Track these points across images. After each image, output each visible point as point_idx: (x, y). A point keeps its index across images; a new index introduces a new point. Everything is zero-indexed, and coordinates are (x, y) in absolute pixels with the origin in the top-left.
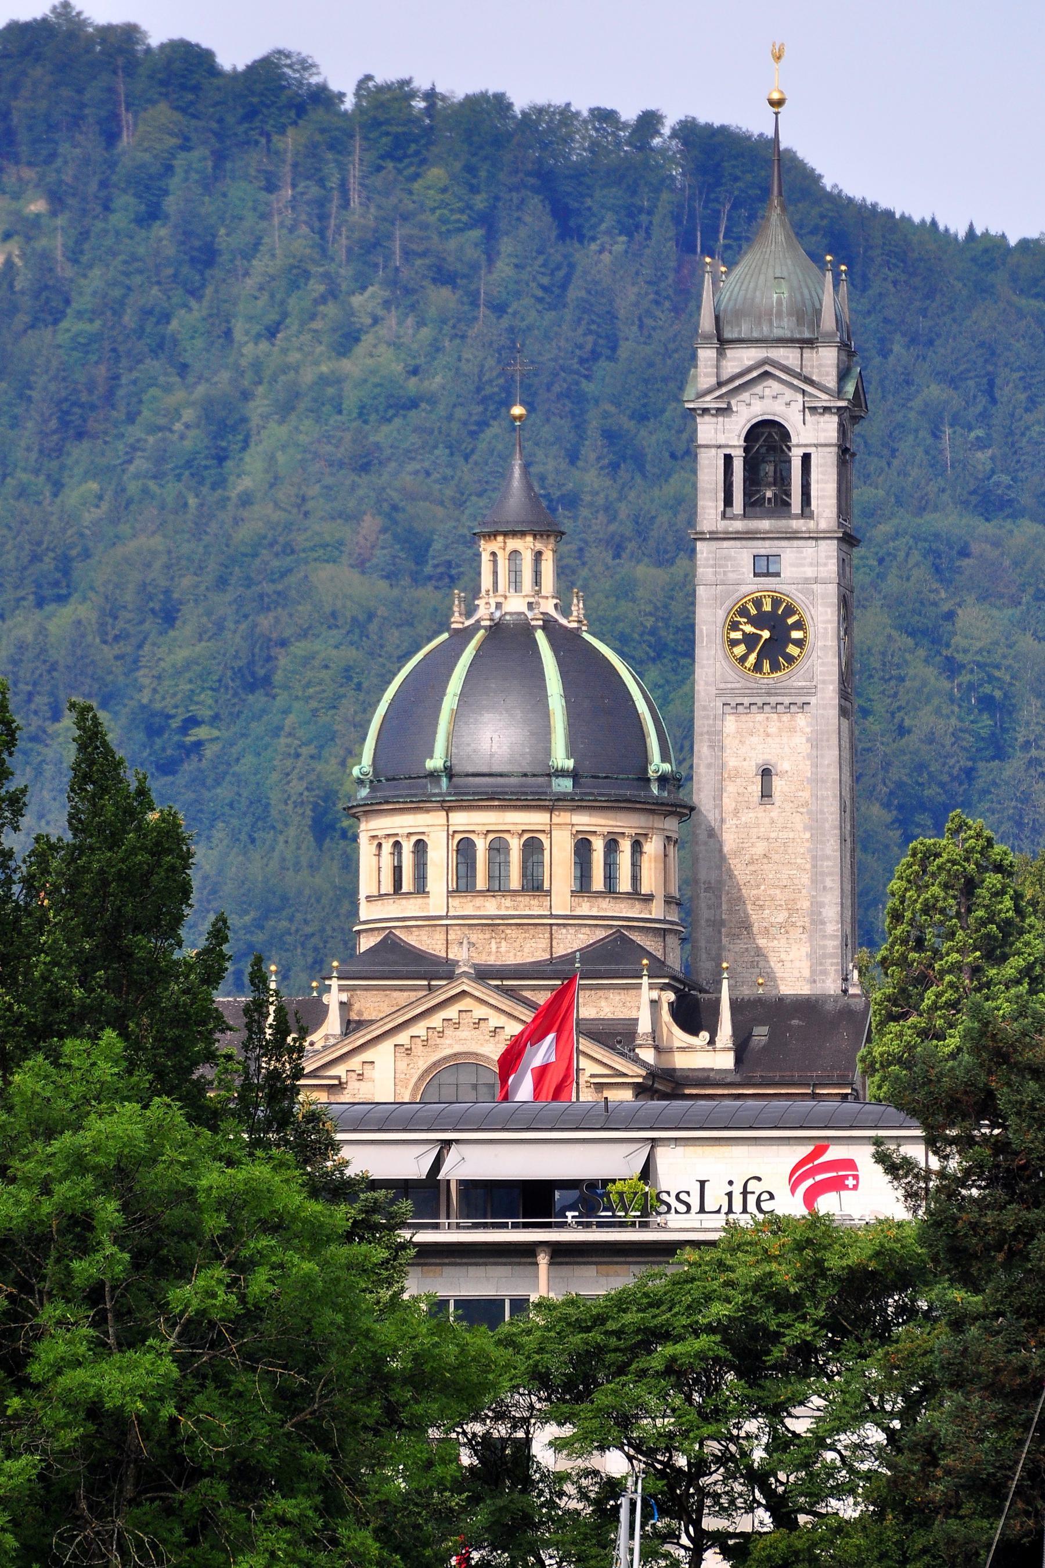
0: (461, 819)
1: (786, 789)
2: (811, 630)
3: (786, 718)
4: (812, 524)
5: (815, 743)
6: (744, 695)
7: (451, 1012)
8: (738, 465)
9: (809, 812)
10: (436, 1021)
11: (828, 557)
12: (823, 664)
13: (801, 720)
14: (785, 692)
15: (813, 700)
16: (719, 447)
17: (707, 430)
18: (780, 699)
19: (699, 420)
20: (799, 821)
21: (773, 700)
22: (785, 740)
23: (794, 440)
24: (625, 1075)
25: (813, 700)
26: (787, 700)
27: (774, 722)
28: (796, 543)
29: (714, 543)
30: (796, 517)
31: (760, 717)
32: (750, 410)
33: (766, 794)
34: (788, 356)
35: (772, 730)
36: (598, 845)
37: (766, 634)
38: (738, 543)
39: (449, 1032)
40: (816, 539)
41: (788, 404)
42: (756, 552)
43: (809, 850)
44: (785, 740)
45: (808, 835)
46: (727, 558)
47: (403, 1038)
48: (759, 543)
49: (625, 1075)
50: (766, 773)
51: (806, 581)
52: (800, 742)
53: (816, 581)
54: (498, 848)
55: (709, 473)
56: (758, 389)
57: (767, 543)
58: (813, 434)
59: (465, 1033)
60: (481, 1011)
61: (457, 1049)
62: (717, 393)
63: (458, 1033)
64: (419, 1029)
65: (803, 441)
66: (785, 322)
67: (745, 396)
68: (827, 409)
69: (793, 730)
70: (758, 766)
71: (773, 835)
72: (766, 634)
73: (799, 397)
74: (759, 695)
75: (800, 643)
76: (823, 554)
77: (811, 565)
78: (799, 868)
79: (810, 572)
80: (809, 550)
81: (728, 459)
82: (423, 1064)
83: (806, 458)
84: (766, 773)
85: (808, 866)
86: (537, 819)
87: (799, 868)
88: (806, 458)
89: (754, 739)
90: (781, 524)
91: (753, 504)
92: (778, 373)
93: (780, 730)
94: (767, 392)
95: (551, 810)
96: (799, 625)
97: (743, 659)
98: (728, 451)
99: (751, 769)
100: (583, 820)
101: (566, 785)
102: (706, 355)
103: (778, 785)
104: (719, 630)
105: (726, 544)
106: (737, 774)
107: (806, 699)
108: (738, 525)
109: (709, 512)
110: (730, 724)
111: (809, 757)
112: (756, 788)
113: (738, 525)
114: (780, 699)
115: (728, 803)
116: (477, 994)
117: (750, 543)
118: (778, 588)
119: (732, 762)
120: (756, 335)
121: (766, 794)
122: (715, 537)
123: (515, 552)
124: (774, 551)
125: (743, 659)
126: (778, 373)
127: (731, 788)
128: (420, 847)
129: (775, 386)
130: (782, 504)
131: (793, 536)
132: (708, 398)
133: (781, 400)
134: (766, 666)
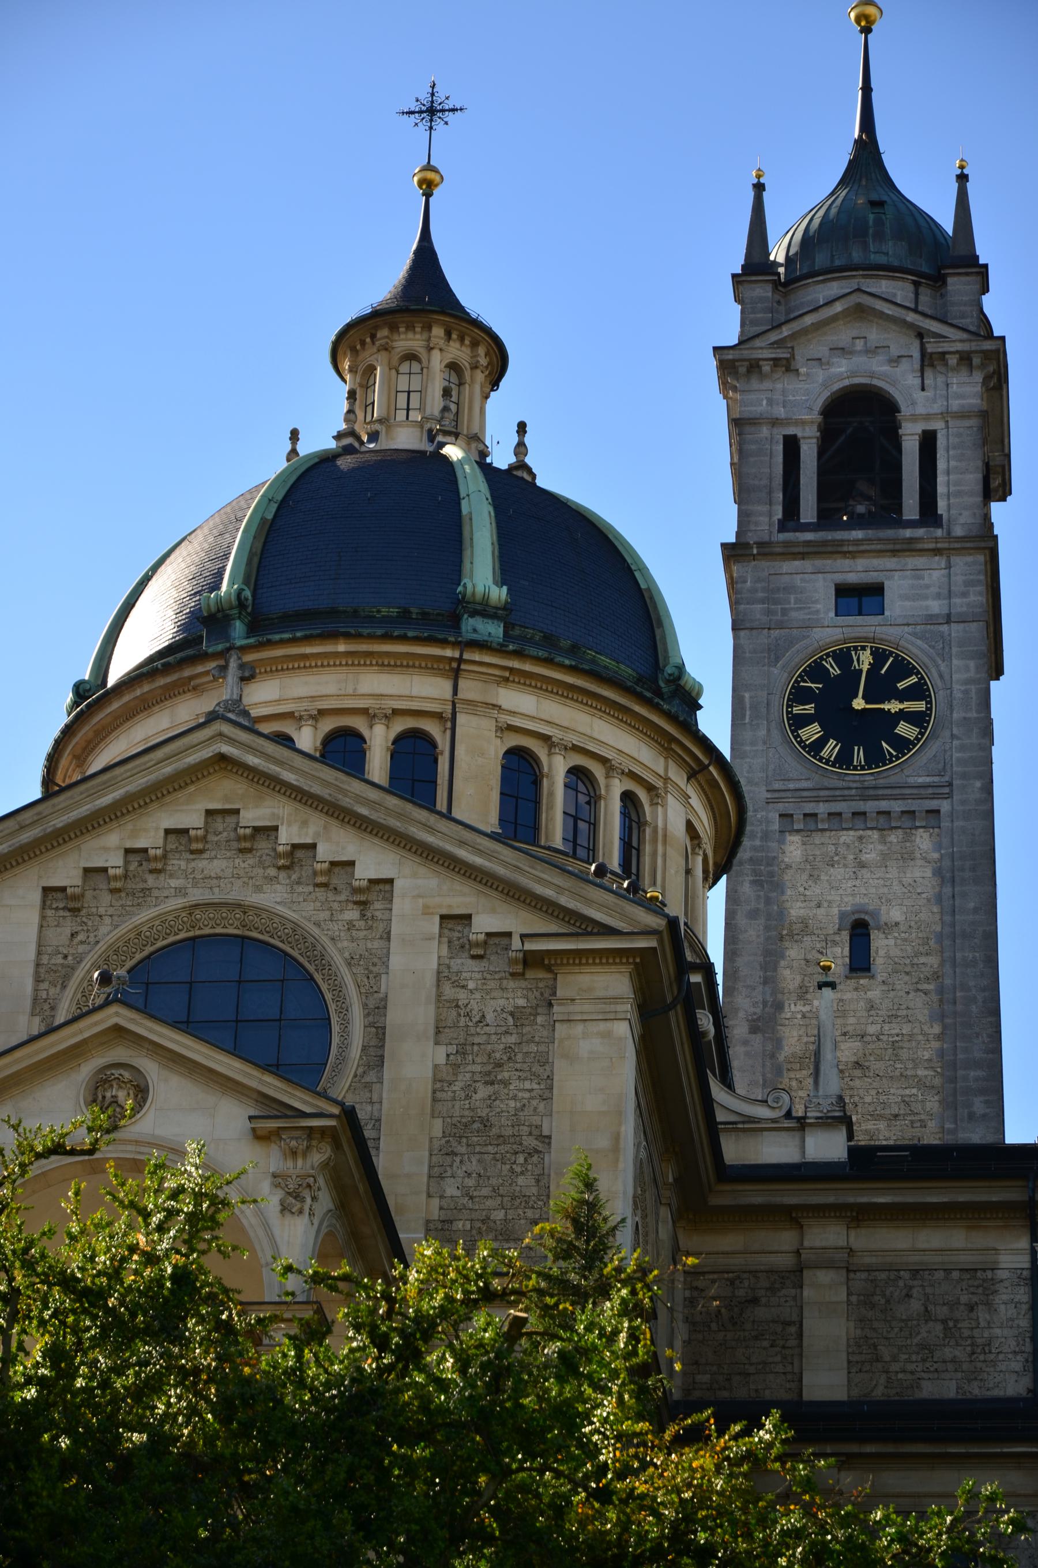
1: (895, 952)
2: (939, 698)
3: (893, 837)
4: (939, 533)
6: (817, 800)
7: (188, 815)
8: (809, 453)
9: (941, 991)
10: (149, 831)
11: (968, 584)
12: (962, 748)
13: (923, 841)
14: (897, 792)
15: (945, 806)
16: (775, 422)
18: (884, 805)
20: (920, 1006)
21: (870, 806)
22: (893, 873)
23: (905, 410)
24: (610, 931)
25: (945, 806)
29: (766, 566)
30: (911, 524)
31: (847, 837)
33: (860, 963)
35: (870, 856)
36: (557, 768)
37: (859, 704)
38: (808, 565)
39: (177, 863)
41: (896, 360)
42: (840, 578)
43: (941, 1054)
44: (893, 873)
45: (937, 1029)
46: (789, 589)
47: (65, 871)
48: (845, 563)
49: (610, 931)
50: (860, 931)
51: (931, 620)
52: (921, 874)
53: (948, 619)
56: (843, 335)
57: (861, 563)
59: (216, 865)
61: (197, 895)
62: (774, 337)
63: (201, 864)
64: (106, 850)
65: (920, 410)
66: (889, 246)
69: (907, 857)
70: (843, 915)
71: (872, 1029)
72: (859, 704)
74: (845, 799)
75: (918, 719)
76: (958, 579)
77: (938, 596)
78: (921, 1084)
79: (936, 607)
80: (934, 573)
81: (791, 445)
82: (109, 933)
83: (928, 442)
84: (860, 931)
85: (937, 1081)
86: (428, 689)
87: (921, 1084)
88: (928, 442)
89: (837, 872)
90: (890, 533)
92: (880, 305)
93: (885, 856)
94: (859, 345)
95: (455, 672)
97: (816, 747)
98: (791, 431)
100: (522, 703)
103: (881, 945)
104: (776, 700)
106: (805, 927)
107: (933, 804)
108: (809, 536)
110: (794, 849)
111: (939, 899)
114: (884, 805)
115: (790, 978)
116: (252, 760)
117: (828, 563)
118: (882, 632)
119: (796, 910)
120: (837, 263)
121: (860, 963)
123: (411, 357)
124: (872, 578)
125: (816, 747)
126: (880, 305)
127: (794, 952)
129: (874, 335)
130: (888, 511)
131: (909, 548)
132: (758, 343)
134: (859, 755)
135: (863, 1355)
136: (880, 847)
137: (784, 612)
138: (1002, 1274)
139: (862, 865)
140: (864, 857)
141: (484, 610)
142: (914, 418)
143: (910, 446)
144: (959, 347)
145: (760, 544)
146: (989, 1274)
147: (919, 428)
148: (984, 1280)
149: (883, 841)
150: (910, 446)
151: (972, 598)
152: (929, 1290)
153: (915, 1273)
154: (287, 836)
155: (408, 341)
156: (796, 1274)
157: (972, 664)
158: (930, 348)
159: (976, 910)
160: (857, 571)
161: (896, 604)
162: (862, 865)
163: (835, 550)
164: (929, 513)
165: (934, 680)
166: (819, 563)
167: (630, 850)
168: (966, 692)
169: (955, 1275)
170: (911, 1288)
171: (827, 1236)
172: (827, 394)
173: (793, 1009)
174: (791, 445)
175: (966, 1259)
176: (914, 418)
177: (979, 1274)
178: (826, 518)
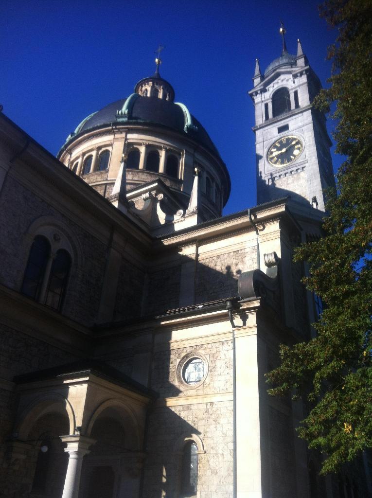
2: (303, 143)
5: (310, 180)
13: (302, 174)
15: (307, 165)
16: (262, 102)
17: (258, 99)
19: (255, 97)
21: (289, 171)
26: (295, 169)
28: (294, 117)
32: (272, 88)
40: (302, 112)
53: (303, 126)
55: (259, 111)
56: (276, 81)
57: (283, 122)
67: (271, 85)
68: (301, 74)
69: (299, 179)
73: (291, 76)
79: (300, 124)
81: (266, 106)
83: (296, 93)
90: (290, 113)
93: (293, 181)
98: (266, 102)
101: (125, 120)
102: (257, 81)
105: (266, 128)
107: (303, 166)
109: (260, 120)
117: (275, 124)
122: (262, 127)
124: (286, 124)
129: (282, 77)
130: (290, 109)
133: (285, 81)
136: (292, 179)
137: (267, 137)
138: (246, 250)
139: (288, 184)
140: (288, 182)
142: (292, 89)
144: (300, 71)
145: (260, 125)
146: (243, 251)
147: (293, 91)
148: (241, 254)
149: (293, 177)
151: (309, 119)
152: (222, 262)
153: (218, 257)
157: (310, 133)
158: (293, 73)
159: (316, 186)
160: (281, 124)
161: (291, 128)
162: (288, 184)
164: (297, 106)
165: (302, 140)
166: (273, 125)
168: (309, 139)
169: (232, 254)
170: (217, 262)
172: (273, 93)
174: (266, 106)
175: (236, 248)
176: (292, 89)
177: (240, 252)
178: (275, 115)
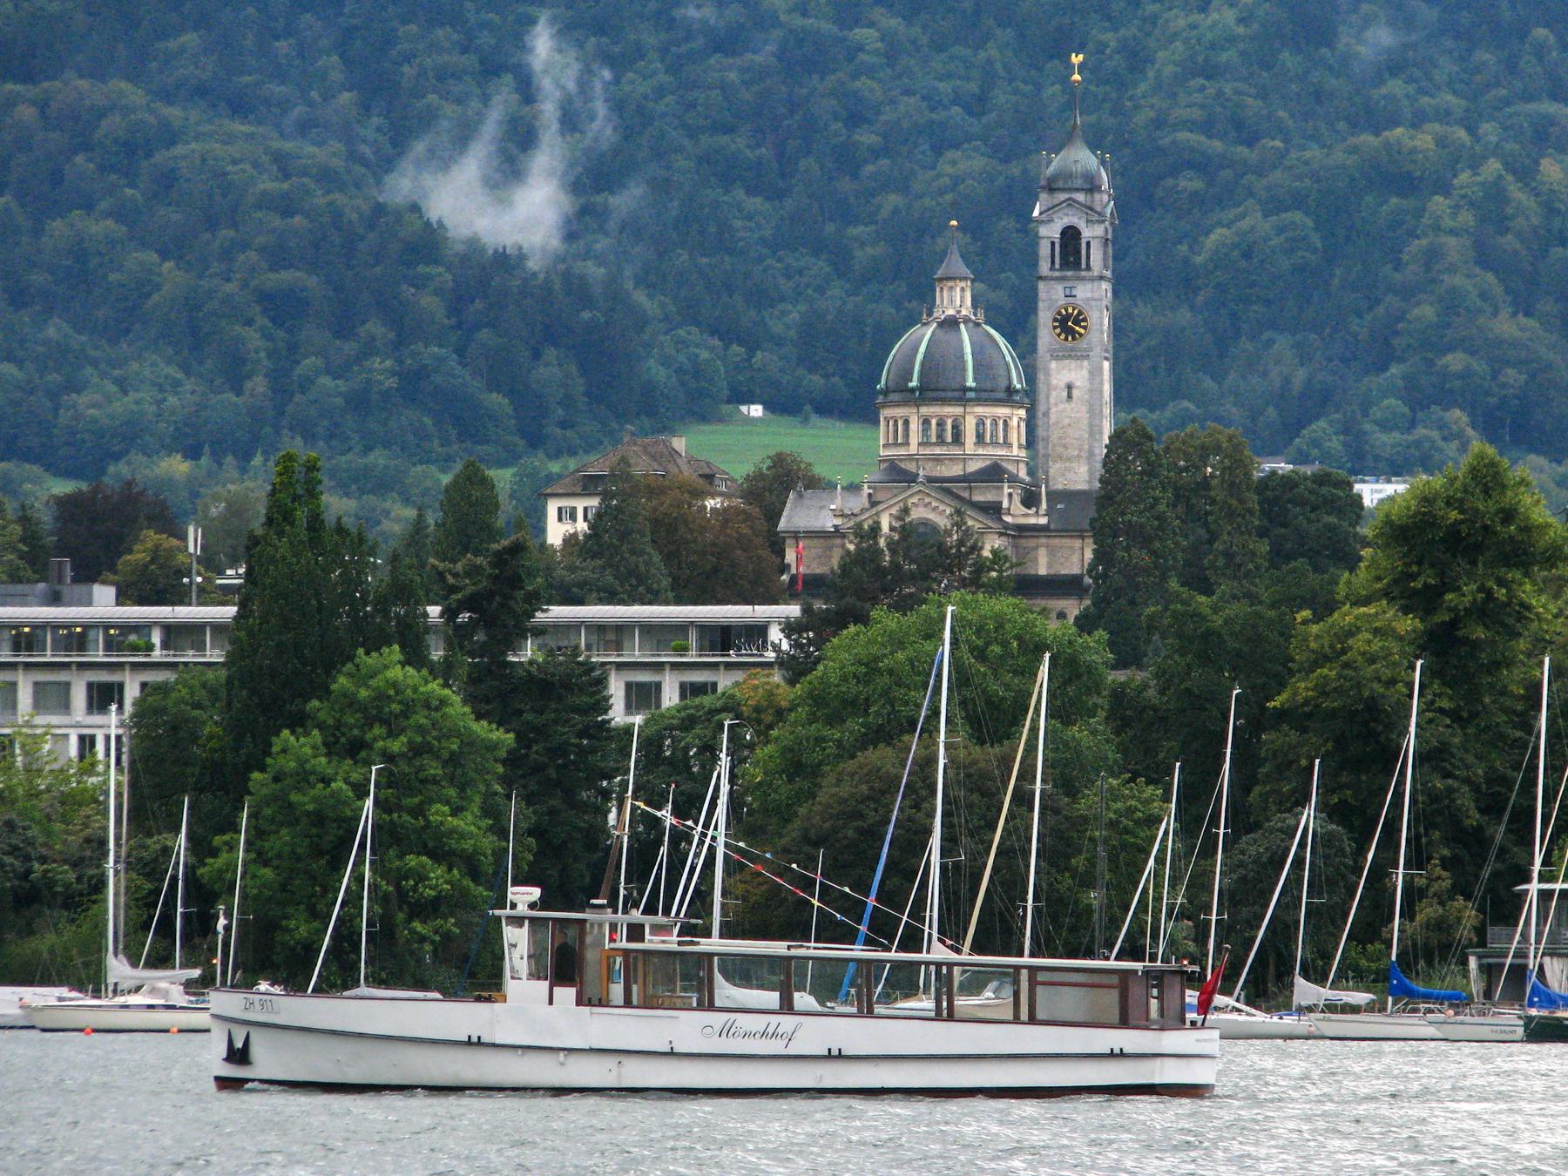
0: (924, 410)
13: (1086, 363)
17: (1043, 231)
20: (1084, 409)
27: (1073, 364)
33: (1070, 397)
34: (1080, 197)
50: (1070, 387)
52: (1085, 373)
54: (941, 424)
55: (1044, 250)
58: (1091, 233)
59: (921, 509)
60: (927, 500)
79: (1089, 295)
80: (1089, 286)
81: (1053, 244)
83: (1088, 244)
84: (1070, 387)
86: (958, 410)
91: (1065, 265)
96: (1085, 320)
99: (1062, 384)
100: (979, 410)
101: (971, 395)
103: (1075, 393)
108: (1057, 274)
109: (1044, 268)
110: (1053, 365)
112: (1065, 394)
113: (1057, 274)
115: (1052, 401)
119: (1054, 382)
121: (1070, 397)
127: (1054, 394)
128: (906, 423)
131: (1083, 279)
135: (1050, 566)
141: (971, 389)
143: (1084, 246)
150: (1084, 246)
154: (934, 504)
155: (951, 283)
156: (1037, 547)
163: (1063, 279)
164: (1088, 268)
167: (1005, 437)
171: (1043, 540)
173: (1053, 410)
